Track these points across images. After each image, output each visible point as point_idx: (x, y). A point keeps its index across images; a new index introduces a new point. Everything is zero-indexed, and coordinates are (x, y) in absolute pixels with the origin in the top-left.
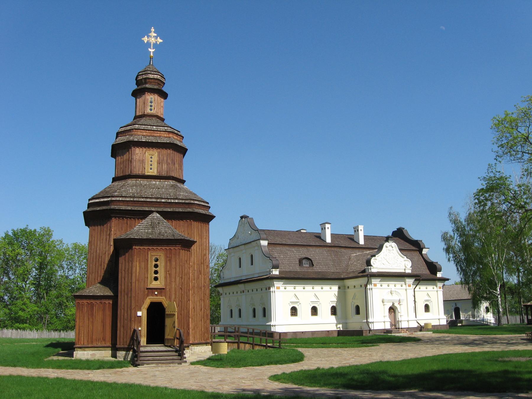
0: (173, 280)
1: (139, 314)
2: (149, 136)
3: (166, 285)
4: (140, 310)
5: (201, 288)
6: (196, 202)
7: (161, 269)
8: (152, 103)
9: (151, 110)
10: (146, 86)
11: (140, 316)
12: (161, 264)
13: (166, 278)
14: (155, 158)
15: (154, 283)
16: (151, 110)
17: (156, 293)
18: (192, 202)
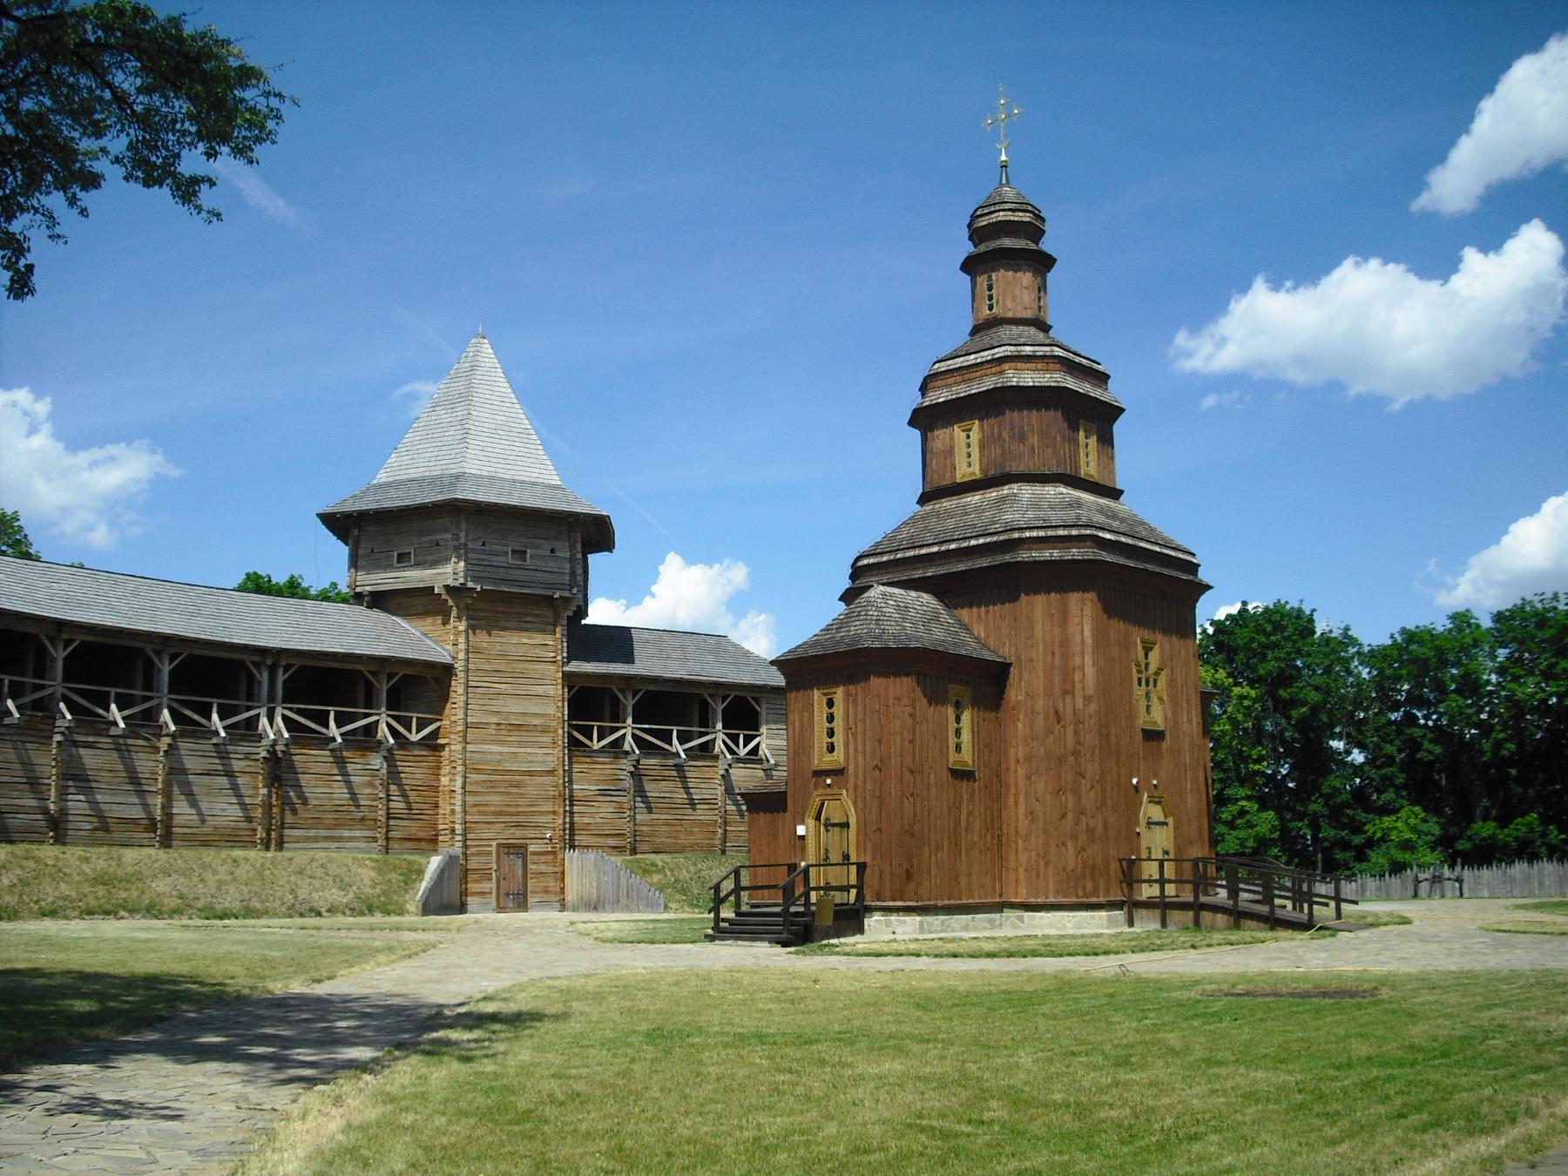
0: (860, 748)
1: (801, 830)
2: (958, 384)
3: (847, 760)
4: (802, 822)
5: (1061, 760)
6: (1028, 534)
7: (838, 725)
8: (1013, 290)
9: (991, 307)
10: (1006, 245)
11: (802, 837)
12: (838, 710)
13: (847, 744)
14: (975, 435)
15: (828, 757)
16: (991, 307)
17: (829, 781)
18: (1016, 535)
